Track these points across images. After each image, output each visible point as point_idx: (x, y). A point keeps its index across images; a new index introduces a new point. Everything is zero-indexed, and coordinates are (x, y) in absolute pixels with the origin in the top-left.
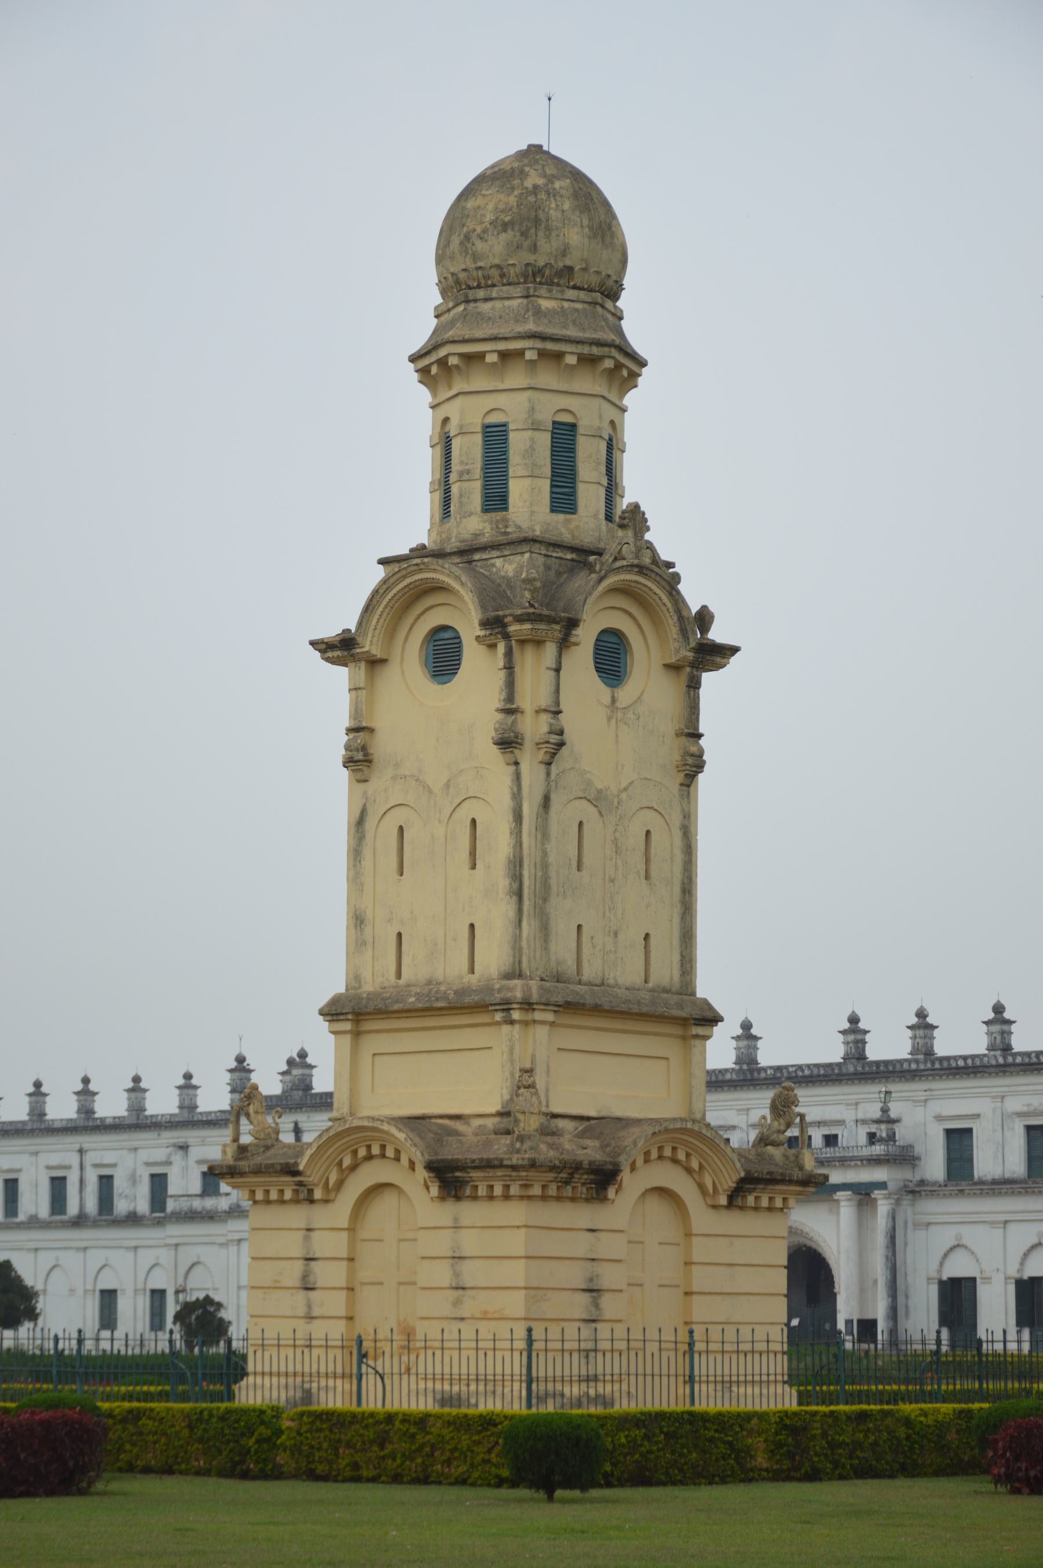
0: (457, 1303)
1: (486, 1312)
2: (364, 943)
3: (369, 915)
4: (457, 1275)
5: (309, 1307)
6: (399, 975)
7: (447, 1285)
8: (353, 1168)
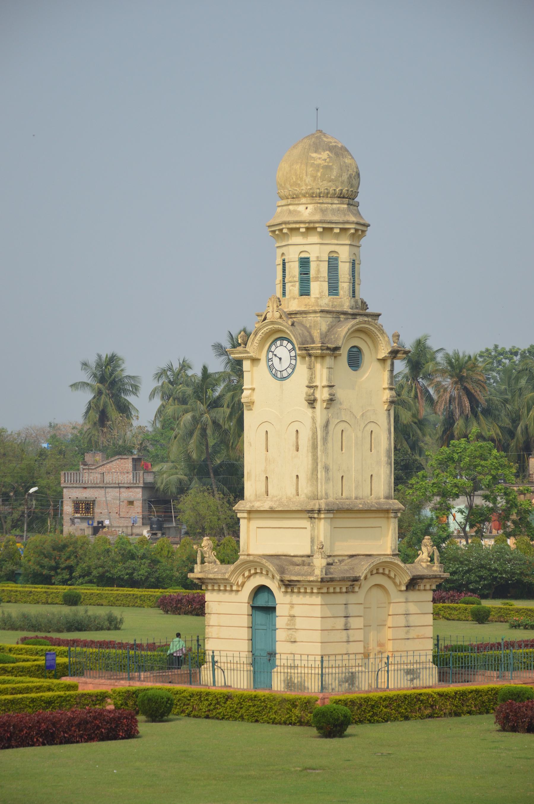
0: (407, 632)
1: (418, 636)
2: (329, 479)
3: (331, 467)
4: (407, 621)
5: (348, 637)
6: (342, 495)
7: (404, 625)
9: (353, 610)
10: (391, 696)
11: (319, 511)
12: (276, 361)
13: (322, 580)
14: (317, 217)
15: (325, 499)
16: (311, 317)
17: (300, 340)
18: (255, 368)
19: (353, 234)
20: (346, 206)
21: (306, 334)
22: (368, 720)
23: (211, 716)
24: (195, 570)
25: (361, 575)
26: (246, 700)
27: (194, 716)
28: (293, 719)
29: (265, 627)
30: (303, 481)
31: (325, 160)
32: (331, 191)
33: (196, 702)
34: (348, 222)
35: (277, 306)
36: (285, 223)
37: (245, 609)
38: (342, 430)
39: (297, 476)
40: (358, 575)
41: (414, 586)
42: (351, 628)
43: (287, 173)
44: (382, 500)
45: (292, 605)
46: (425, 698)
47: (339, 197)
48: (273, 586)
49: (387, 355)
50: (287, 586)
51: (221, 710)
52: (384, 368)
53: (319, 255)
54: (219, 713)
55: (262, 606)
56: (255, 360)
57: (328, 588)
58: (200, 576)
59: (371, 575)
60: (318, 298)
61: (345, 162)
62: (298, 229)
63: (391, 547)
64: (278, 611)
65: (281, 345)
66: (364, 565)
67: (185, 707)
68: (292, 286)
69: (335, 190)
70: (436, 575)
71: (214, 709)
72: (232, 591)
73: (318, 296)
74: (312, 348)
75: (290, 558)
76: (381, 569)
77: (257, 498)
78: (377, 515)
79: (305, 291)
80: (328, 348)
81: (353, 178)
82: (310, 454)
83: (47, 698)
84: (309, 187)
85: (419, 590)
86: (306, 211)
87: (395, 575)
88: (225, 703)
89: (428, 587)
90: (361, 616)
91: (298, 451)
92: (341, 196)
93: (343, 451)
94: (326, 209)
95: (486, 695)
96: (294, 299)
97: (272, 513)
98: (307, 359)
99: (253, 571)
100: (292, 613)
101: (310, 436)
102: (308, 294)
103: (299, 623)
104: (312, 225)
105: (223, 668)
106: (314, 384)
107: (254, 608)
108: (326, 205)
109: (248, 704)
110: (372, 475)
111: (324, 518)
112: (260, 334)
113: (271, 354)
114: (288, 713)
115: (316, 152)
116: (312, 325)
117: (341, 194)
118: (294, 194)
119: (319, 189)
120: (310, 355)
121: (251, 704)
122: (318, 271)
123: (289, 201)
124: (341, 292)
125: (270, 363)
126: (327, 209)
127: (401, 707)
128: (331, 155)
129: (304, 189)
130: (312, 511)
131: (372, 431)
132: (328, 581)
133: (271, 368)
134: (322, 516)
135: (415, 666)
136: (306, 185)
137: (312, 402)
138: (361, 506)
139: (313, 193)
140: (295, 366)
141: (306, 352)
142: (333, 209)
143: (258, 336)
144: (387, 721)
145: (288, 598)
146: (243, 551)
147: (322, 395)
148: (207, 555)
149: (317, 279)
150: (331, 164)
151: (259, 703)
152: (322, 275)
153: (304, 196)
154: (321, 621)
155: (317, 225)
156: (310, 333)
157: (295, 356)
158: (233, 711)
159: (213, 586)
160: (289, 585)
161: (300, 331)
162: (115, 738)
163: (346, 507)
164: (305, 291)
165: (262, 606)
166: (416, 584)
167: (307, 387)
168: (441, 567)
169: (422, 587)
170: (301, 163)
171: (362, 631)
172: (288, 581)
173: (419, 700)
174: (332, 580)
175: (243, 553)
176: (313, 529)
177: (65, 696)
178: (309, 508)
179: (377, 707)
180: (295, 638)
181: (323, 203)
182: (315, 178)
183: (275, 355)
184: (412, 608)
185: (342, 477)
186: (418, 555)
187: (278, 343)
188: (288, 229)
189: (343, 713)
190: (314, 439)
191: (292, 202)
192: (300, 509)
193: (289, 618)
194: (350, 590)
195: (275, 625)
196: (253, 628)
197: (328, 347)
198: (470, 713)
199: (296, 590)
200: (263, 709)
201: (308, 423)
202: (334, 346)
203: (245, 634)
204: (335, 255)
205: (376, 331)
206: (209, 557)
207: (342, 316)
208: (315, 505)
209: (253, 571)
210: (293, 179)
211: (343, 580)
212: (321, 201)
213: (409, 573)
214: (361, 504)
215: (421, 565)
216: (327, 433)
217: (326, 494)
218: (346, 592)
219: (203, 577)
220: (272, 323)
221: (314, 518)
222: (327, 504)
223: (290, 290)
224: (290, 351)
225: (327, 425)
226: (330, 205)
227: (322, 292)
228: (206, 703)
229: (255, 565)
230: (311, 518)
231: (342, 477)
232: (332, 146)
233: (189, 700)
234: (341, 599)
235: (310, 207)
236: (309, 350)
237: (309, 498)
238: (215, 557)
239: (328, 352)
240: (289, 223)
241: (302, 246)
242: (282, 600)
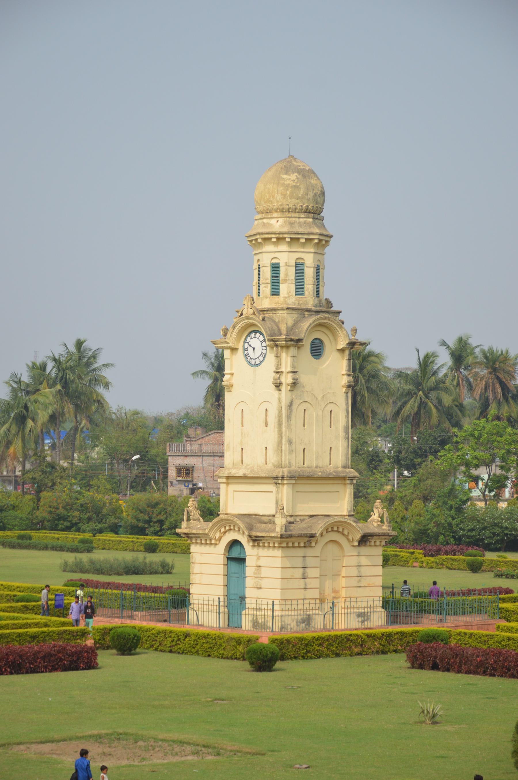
0: (359, 581)
1: (369, 584)
2: (292, 451)
3: (294, 441)
4: (359, 572)
5: (306, 585)
6: (304, 464)
7: (356, 575)
8: (225, 533)
9: (310, 562)
10: (323, 636)
11: (283, 478)
12: (250, 350)
13: (282, 536)
14: (285, 229)
15: (289, 467)
16: (279, 314)
17: (269, 332)
18: (234, 356)
19: (317, 244)
20: (311, 220)
21: (275, 327)
22: (302, 657)
23: (173, 650)
24: (182, 527)
25: (316, 532)
26: (201, 638)
27: (161, 651)
28: (238, 654)
30: (271, 453)
31: (294, 181)
32: (299, 207)
33: (162, 638)
34: (312, 234)
35: (252, 304)
36: (259, 234)
37: (221, 559)
38: (305, 410)
39: (266, 448)
40: (314, 533)
41: (365, 542)
42: (309, 577)
43: (262, 192)
44: (340, 469)
45: (258, 557)
46: (354, 638)
47: (306, 212)
48: (244, 540)
49: (345, 346)
50: (254, 541)
51: (181, 646)
52: (343, 357)
53: (287, 261)
54: (180, 648)
55: (235, 558)
56: (234, 350)
57: (287, 543)
58: (185, 531)
59: (327, 532)
60: (286, 297)
61: (310, 183)
62: (270, 239)
63: (347, 509)
64: (248, 562)
65: (255, 337)
66: (320, 523)
67: (154, 643)
68: (265, 287)
69: (301, 206)
70: (384, 533)
71: (176, 645)
72: (211, 544)
73: (286, 296)
74: (279, 340)
75: (259, 517)
76: (336, 527)
77: (234, 466)
78: (336, 482)
79: (275, 292)
80: (292, 340)
81: (317, 196)
82: (276, 430)
83: (32, 633)
84: (280, 204)
85: (370, 546)
86: (277, 224)
87: (348, 533)
88: (184, 640)
89: (378, 543)
90: (317, 567)
91: (267, 426)
92: (307, 212)
93: (306, 427)
94: (294, 223)
95: (410, 636)
96: (267, 298)
97: (245, 479)
98: (274, 348)
99: (227, 528)
100: (259, 564)
101: (277, 415)
102: (278, 294)
103: (264, 572)
104: (281, 236)
105: (195, 609)
106: (280, 370)
107: (229, 559)
108: (294, 219)
109: (202, 641)
110: (331, 448)
111: (287, 484)
112: (238, 327)
113: (246, 344)
114: (234, 649)
115: (286, 174)
116: (280, 320)
117: (307, 209)
118: (268, 209)
119: (288, 205)
120: (277, 346)
121: (204, 641)
122: (287, 275)
123: (263, 215)
124: (306, 293)
125: (246, 352)
126: (295, 222)
127: (333, 646)
128: (299, 176)
129: (276, 205)
130: (276, 478)
131: (331, 411)
132: (287, 537)
133: (246, 356)
134: (285, 482)
135: (366, 610)
136: (278, 202)
137: (278, 385)
138: (320, 474)
139: (283, 209)
140: (266, 354)
141: (273, 343)
142: (300, 222)
143: (236, 329)
144: (319, 657)
145: (255, 551)
146: (223, 511)
147: (287, 379)
148: (192, 514)
149: (285, 281)
150: (298, 184)
151: (211, 640)
152: (290, 278)
153: (276, 211)
154: (281, 571)
155: (285, 236)
156: (278, 327)
158: (190, 647)
159: (196, 540)
160: (255, 540)
161: (270, 326)
162: (77, 669)
163: (306, 474)
164: (275, 292)
165: (235, 558)
166: (367, 540)
167: (275, 372)
168: (389, 526)
169: (372, 543)
170: (274, 183)
171: (318, 579)
173: (348, 640)
174: (290, 536)
175: (223, 513)
176: (278, 492)
177: (48, 631)
178: (274, 475)
179: (311, 645)
180: (260, 585)
181: (291, 217)
182: (284, 196)
183: (250, 346)
184: (364, 561)
185: (304, 449)
186: (371, 516)
187: (253, 335)
188: (262, 239)
189: (271, 650)
191: (266, 216)
192: (267, 475)
194: (308, 545)
195: (245, 574)
196: (228, 575)
197: (291, 339)
198: (396, 651)
199: (261, 544)
200: (214, 646)
201: (275, 403)
202: (297, 338)
203: (221, 580)
204: (301, 261)
205: (335, 326)
206: (194, 515)
207: (307, 313)
208: (279, 472)
209: (227, 528)
211: (300, 536)
212: (290, 216)
213: (360, 531)
214: (320, 472)
215: (373, 525)
216: (291, 412)
217: (290, 463)
218: (305, 547)
219: (188, 532)
220: (247, 318)
221: (279, 483)
222: (289, 472)
223: (263, 291)
224: (261, 342)
225: (291, 405)
226: (297, 219)
227: (290, 292)
228: (170, 639)
229: (230, 524)
230: (276, 483)
231: (304, 449)
232: (301, 169)
233: (156, 637)
234: (300, 552)
235: (281, 220)
237: (275, 467)
238: (199, 516)
239: (292, 343)
240: (262, 234)
242: (251, 552)
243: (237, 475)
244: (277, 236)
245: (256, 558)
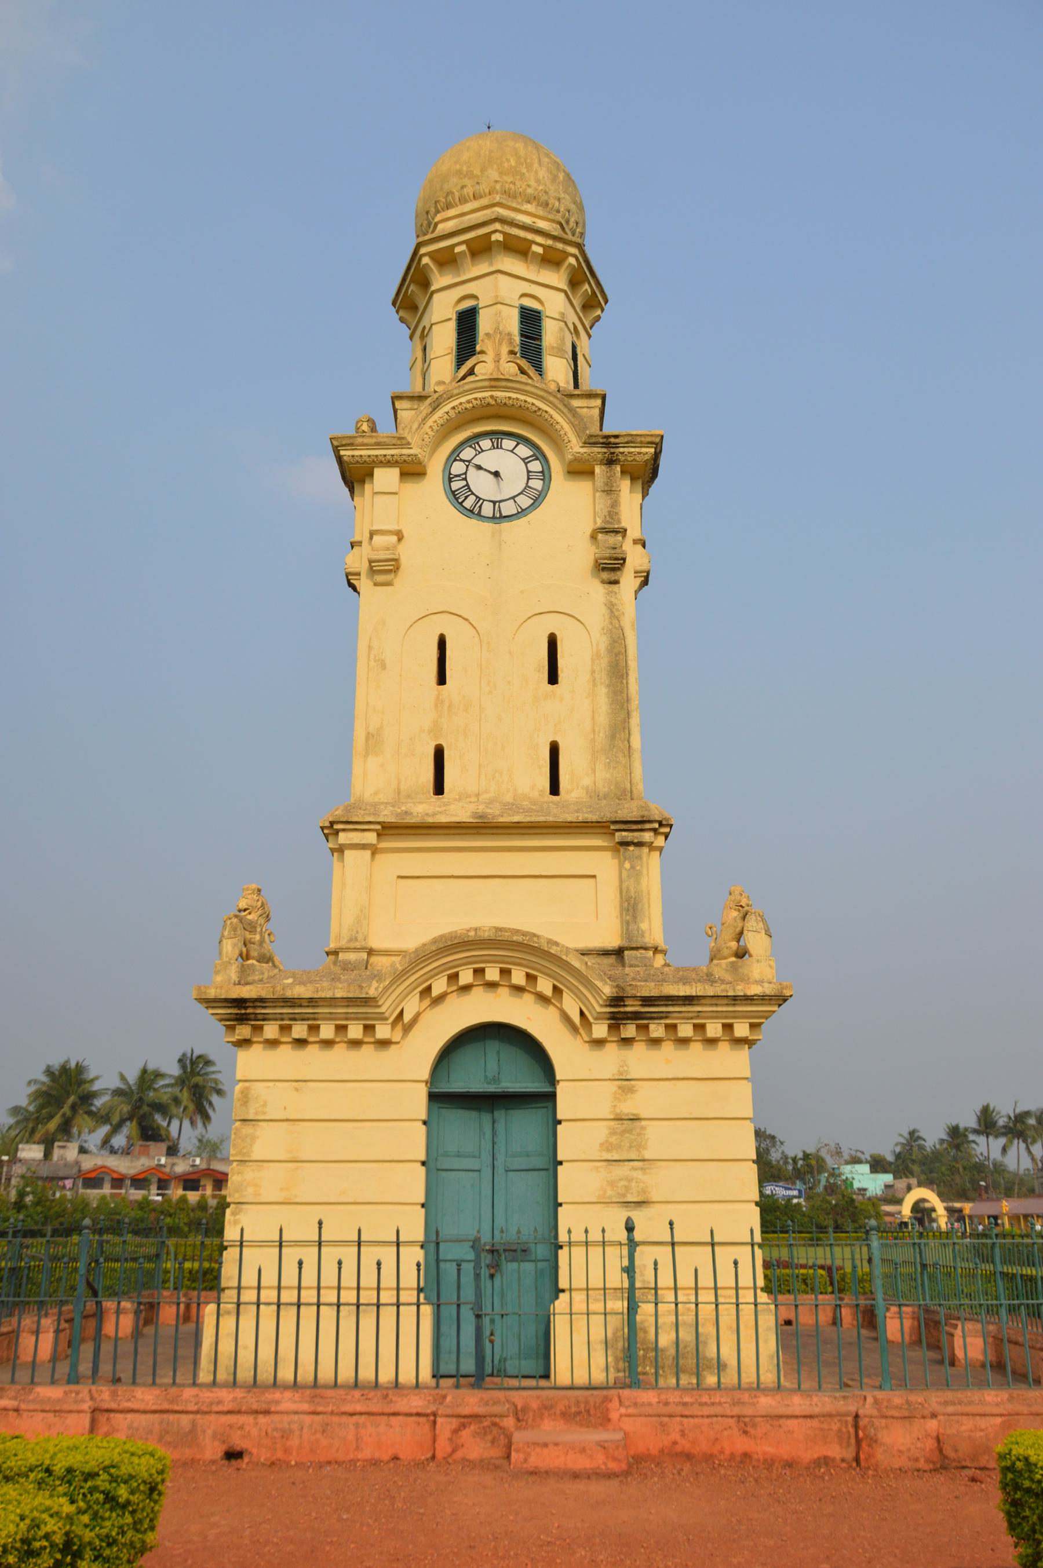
29: (473, 1164)
37: (417, 1102)
82: (602, 692)
100: (628, 1107)
103: (657, 1140)
107: (434, 1097)
112: (447, 408)
136: (538, 181)
137: (610, 568)
143: (440, 413)
157: (542, 472)
172: (647, 1001)
180: (644, 1191)
183: (479, 467)
190: (619, 653)
191: (504, 202)
193: (612, 1123)
201: (596, 616)
210: (508, 161)
230: (625, 844)
236: (616, 445)
240: (512, 224)
241: (527, 284)
243: (444, 819)
244: (550, 242)
245: (612, 1087)
